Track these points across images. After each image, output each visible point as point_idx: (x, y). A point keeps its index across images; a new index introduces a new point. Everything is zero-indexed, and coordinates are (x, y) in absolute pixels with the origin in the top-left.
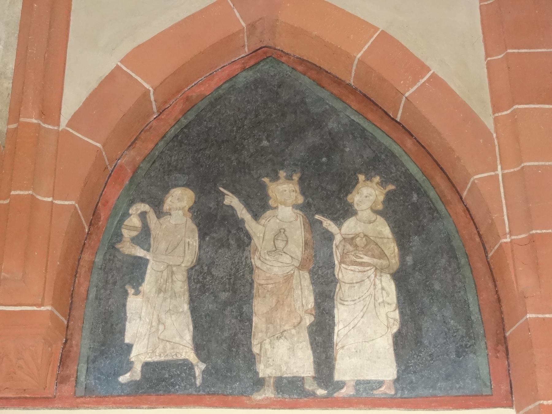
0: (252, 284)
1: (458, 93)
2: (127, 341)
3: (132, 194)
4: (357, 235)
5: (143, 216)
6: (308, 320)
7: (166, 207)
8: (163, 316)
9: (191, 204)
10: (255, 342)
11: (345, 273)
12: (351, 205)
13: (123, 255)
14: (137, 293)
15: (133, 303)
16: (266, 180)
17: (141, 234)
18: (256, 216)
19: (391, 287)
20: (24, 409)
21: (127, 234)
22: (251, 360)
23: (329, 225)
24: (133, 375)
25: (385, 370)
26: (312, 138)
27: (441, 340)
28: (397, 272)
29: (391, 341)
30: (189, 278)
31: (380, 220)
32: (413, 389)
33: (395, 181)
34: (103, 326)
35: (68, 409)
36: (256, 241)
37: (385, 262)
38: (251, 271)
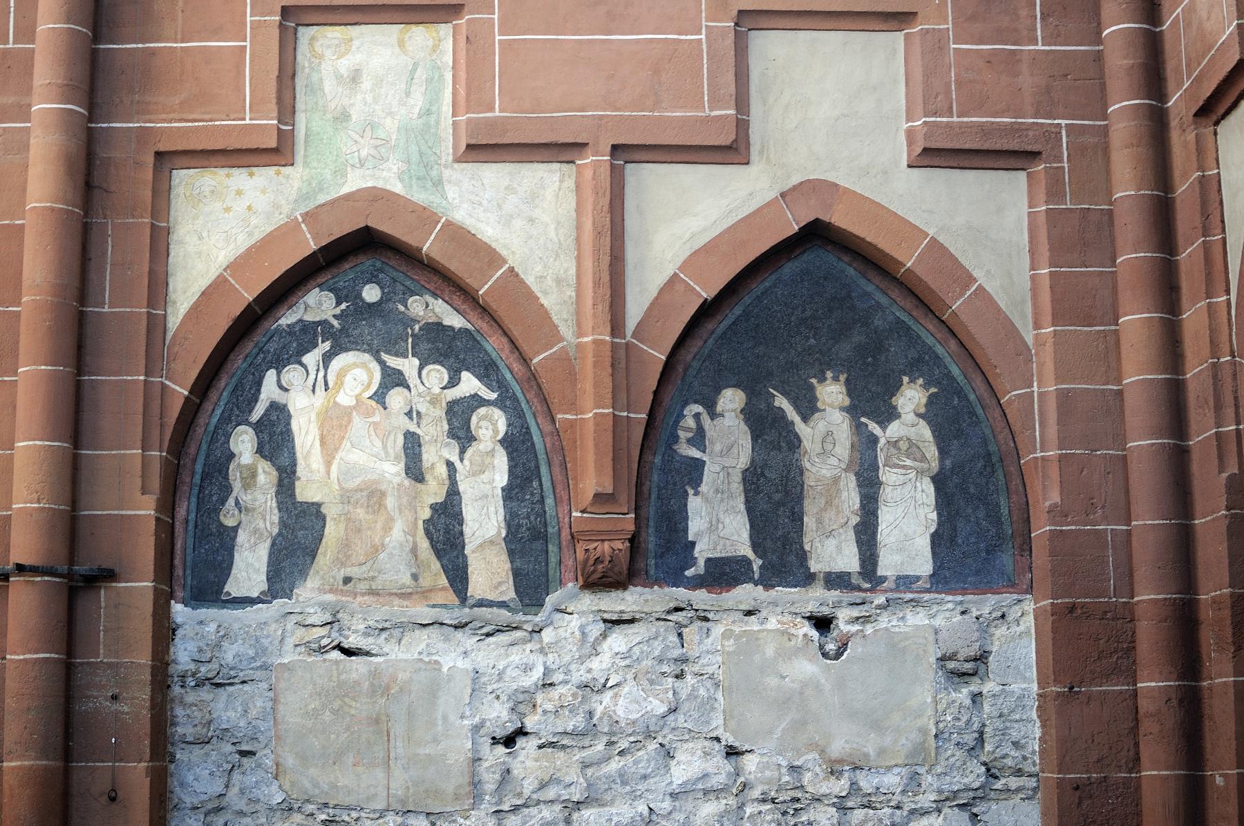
0: (802, 486)
1: (1002, 305)
4: (901, 439)
5: (697, 416)
6: (855, 520)
7: (719, 409)
8: (721, 516)
9: (743, 405)
10: (806, 540)
11: (888, 476)
12: (895, 408)
14: (697, 494)
15: (694, 503)
16: (814, 381)
18: (805, 419)
19: (930, 489)
21: (682, 434)
22: (803, 556)
23: (874, 428)
25: (924, 566)
26: (858, 337)
27: (973, 540)
28: (937, 475)
29: (928, 540)
30: (744, 479)
31: (922, 423)
32: (947, 583)
33: (937, 383)
36: (806, 444)
37: (926, 466)
38: (802, 474)
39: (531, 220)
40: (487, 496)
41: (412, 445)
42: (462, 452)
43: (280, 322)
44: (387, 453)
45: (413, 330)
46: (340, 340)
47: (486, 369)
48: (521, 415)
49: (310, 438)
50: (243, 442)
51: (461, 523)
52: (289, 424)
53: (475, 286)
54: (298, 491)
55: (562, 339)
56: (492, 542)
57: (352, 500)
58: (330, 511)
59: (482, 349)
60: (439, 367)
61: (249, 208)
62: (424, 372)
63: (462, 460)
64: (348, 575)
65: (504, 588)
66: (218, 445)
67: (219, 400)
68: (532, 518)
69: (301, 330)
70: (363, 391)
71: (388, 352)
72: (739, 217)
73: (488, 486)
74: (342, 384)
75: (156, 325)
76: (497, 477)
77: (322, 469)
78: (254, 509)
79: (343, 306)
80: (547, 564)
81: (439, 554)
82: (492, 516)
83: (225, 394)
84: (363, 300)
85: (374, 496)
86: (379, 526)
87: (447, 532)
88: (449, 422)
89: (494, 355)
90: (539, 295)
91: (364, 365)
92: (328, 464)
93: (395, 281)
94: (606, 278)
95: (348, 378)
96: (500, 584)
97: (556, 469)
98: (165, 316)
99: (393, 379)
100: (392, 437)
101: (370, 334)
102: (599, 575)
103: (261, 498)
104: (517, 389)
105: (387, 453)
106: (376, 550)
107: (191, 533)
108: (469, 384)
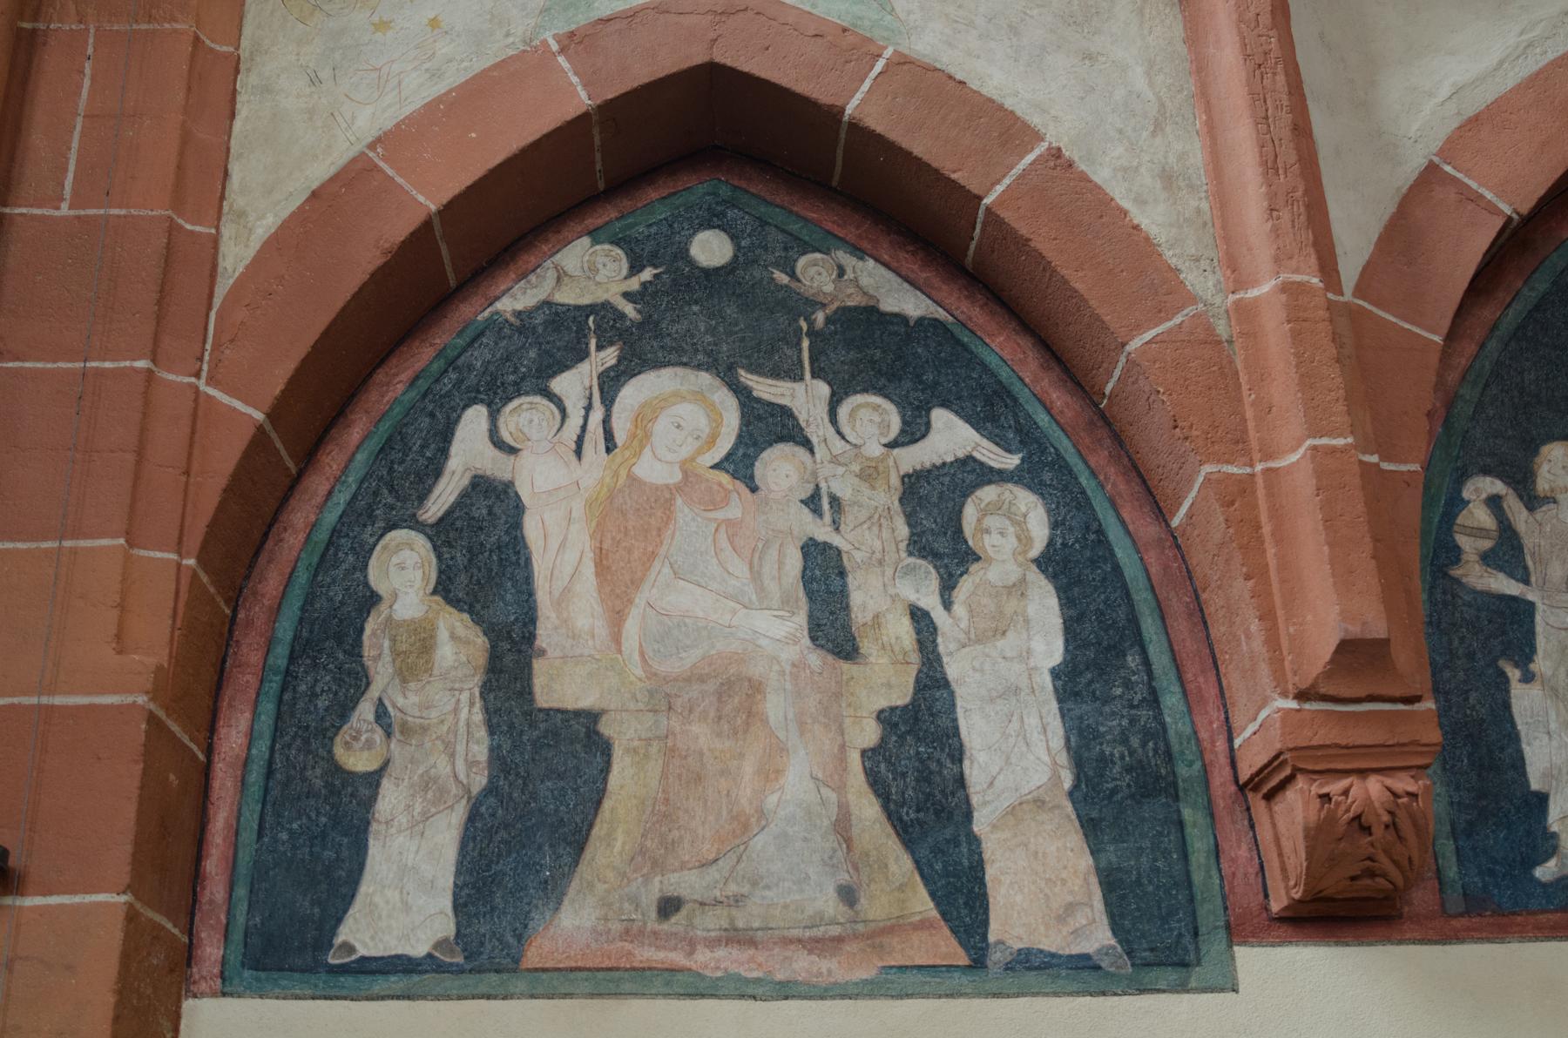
2: (1535, 785)
3: (1458, 457)
5: (1494, 502)
7: (1542, 485)
13: (1474, 591)
14: (1528, 678)
15: (1525, 700)
17: (1499, 545)
20: (1337, 944)
24: (1563, 865)
34: (1470, 755)
35: (1436, 942)
39: (1089, 57)
40: (1017, 691)
41: (824, 575)
42: (947, 588)
43: (499, 305)
44: (761, 589)
45: (811, 323)
46: (641, 344)
47: (989, 402)
48: (1082, 503)
49: (571, 557)
50: (401, 567)
51: (958, 755)
52: (516, 525)
53: (974, 187)
54: (539, 682)
55: (1192, 299)
56: (1039, 803)
57: (678, 703)
58: (621, 732)
59: (974, 361)
60: (878, 400)
61: (434, 23)
62: (843, 411)
63: (947, 605)
64: (672, 891)
65: (1080, 919)
66: (340, 573)
67: (345, 469)
68: (1135, 742)
69: (546, 323)
70: (700, 452)
71: (753, 369)
72: (1550, 56)
73: (1017, 667)
74: (648, 436)
75: (184, 260)
76: (1038, 645)
77: (602, 630)
78: (425, 729)
79: (647, 274)
80: (1185, 857)
81: (907, 833)
82: (1035, 736)
83: (359, 457)
84: (691, 262)
85: (734, 693)
86: (748, 768)
87: (925, 777)
88: (911, 519)
89: (1004, 374)
90: (1125, 204)
91: (699, 397)
92: (617, 619)
93: (763, 223)
94: (1288, 155)
95: (662, 426)
96: (1071, 908)
97: (1182, 627)
98: (215, 241)
99: (768, 427)
100: (773, 553)
101: (712, 331)
102: (1356, 869)
103: (443, 701)
104: (1065, 446)
105: (761, 589)
106: (744, 826)
107: (255, 790)
108: (952, 436)
